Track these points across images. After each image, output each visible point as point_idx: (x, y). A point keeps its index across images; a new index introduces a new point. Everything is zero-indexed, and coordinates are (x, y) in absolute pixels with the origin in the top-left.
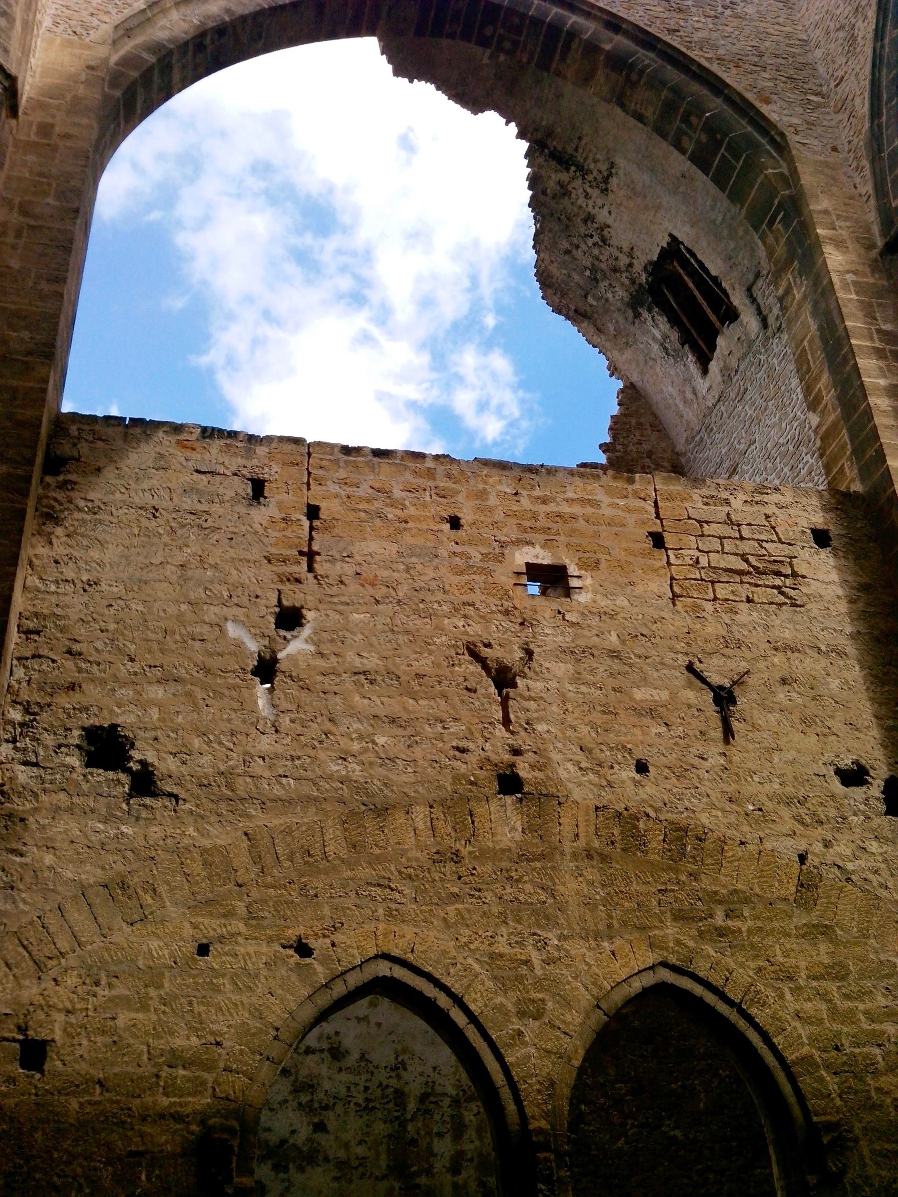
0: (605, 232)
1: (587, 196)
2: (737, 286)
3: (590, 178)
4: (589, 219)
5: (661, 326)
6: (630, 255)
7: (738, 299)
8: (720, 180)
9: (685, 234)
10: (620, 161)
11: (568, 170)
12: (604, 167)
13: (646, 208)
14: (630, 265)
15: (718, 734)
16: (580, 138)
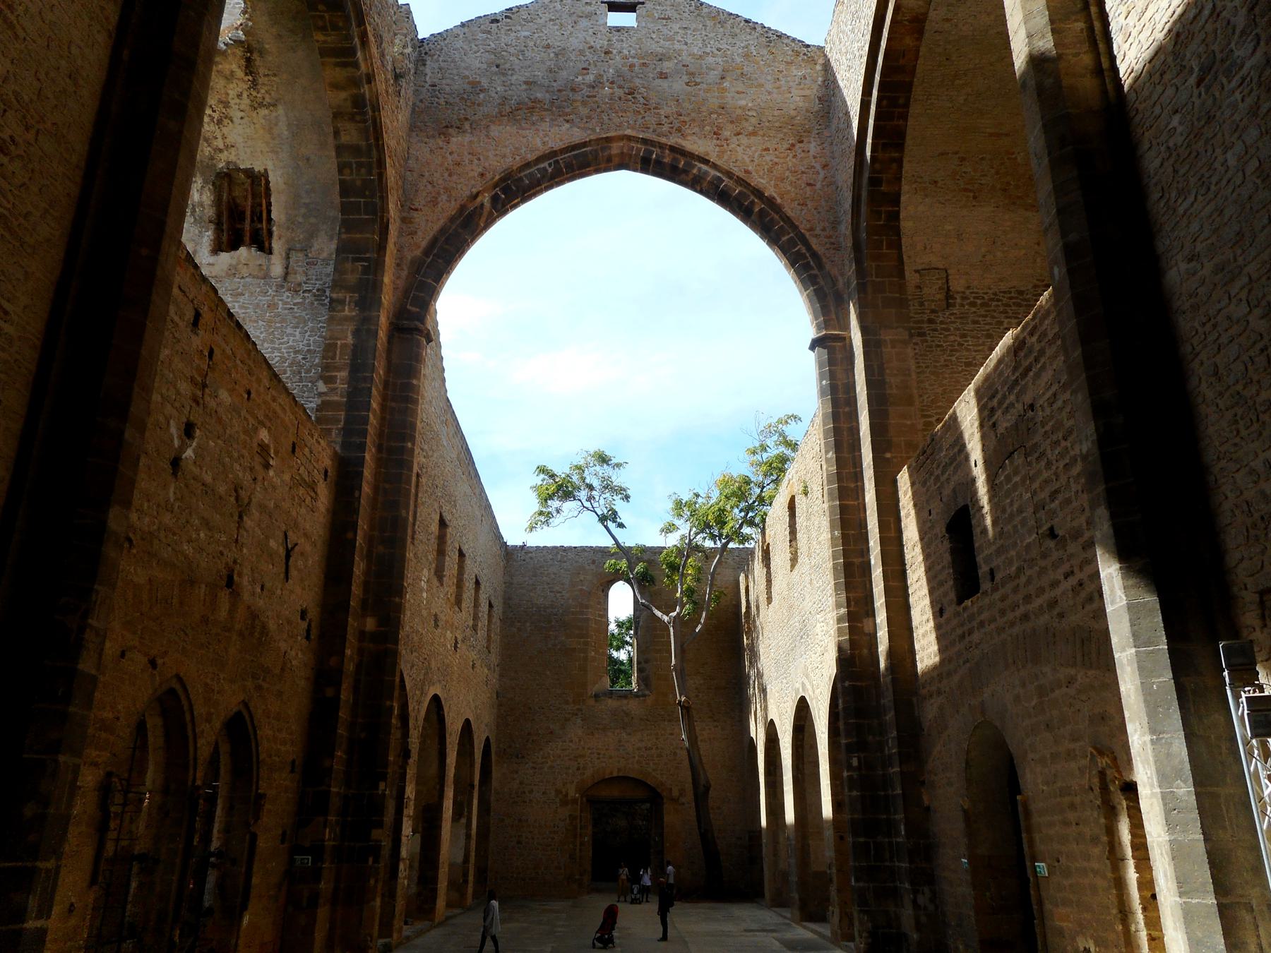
0: (226, 121)
1: (240, 96)
2: (283, 240)
3: (254, 94)
4: (226, 104)
5: (204, 198)
6: (227, 147)
7: (276, 245)
8: (345, 208)
9: (276, 180)
10: (281, 110)
11: (246, 74)
12: (268, 99)
13: (267, 143)
14: (221, 151)
15: (282, 576)
16: (275, 75)
